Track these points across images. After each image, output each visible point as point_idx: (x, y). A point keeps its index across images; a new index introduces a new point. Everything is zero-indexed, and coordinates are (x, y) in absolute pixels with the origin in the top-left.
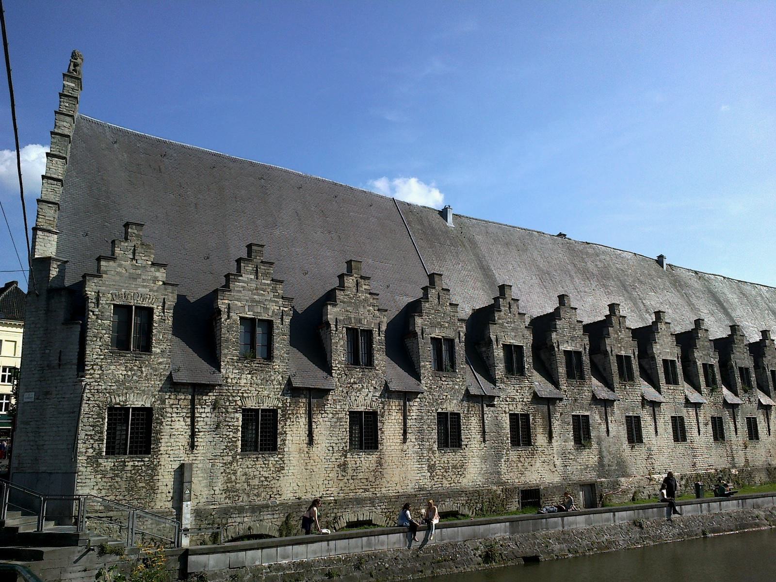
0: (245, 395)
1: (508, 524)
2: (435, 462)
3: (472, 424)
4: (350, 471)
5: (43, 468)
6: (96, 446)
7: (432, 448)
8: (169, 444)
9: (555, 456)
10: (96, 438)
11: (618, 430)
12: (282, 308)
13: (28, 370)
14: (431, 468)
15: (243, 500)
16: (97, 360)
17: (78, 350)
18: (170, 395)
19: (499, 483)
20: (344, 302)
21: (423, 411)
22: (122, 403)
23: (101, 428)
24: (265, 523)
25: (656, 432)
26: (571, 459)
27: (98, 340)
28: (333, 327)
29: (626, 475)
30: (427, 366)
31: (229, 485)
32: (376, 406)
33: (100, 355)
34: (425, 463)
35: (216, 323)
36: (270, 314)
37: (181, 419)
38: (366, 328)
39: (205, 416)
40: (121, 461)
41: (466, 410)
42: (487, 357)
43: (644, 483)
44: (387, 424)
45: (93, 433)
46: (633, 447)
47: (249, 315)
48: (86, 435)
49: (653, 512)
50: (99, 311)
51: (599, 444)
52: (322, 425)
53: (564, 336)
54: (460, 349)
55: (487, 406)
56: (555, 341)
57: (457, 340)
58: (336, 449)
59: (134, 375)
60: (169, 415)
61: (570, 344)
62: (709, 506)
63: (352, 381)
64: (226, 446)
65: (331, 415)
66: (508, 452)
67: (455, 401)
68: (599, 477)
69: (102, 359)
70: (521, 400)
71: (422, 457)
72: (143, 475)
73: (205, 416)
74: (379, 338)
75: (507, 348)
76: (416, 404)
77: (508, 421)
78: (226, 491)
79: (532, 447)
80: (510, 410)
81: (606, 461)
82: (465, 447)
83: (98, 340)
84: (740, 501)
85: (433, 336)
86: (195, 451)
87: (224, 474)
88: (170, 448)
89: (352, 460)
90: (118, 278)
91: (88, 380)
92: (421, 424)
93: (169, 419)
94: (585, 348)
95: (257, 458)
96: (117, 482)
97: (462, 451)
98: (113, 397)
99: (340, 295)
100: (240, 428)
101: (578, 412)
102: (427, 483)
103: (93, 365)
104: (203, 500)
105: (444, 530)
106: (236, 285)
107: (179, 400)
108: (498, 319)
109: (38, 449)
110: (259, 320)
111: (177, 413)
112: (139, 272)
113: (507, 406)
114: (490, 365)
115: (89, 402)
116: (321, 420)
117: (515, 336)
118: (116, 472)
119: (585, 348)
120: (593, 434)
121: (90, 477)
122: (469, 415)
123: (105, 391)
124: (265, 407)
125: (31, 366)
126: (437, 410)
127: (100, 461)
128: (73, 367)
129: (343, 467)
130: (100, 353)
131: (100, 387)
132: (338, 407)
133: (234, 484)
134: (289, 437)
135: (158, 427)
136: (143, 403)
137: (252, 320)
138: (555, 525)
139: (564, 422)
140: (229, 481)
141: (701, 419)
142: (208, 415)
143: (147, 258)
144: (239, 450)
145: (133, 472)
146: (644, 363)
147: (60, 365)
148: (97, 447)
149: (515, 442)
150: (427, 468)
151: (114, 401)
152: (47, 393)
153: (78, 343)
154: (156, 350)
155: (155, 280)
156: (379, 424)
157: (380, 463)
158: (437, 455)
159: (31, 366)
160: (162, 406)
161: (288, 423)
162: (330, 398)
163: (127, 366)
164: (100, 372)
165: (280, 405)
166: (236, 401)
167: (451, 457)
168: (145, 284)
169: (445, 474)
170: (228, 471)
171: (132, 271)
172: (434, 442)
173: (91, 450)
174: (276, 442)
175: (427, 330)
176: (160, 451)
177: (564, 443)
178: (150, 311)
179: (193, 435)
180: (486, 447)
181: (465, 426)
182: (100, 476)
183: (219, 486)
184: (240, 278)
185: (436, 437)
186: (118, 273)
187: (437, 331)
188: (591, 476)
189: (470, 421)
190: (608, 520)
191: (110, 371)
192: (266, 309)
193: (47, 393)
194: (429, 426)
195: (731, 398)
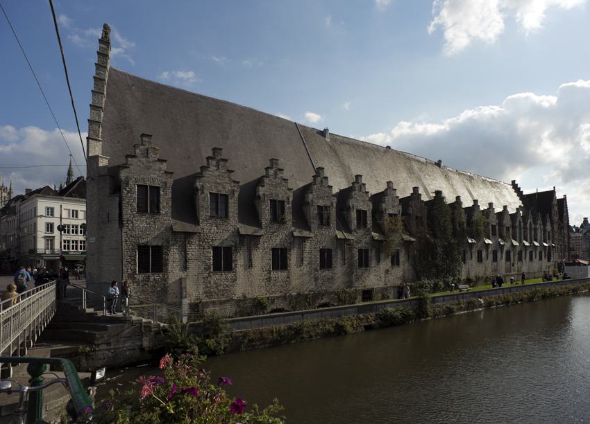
6: (132, 267)
14: (316, 279)
20: (268, 184)
28: (262, 199)
30: (315, 224)
39: (193, 249)
45: (130, 260)
74: (288, 206)
75: (359, 212)
78: (205, 293)
89: (274, 274)
99: (266, 180)
106: (207, 173)
112: (151, 164)
129: (269, 279)
137: (217, 194)
140: (207, 287)
147: (108, 221)
149: (360, 265)
154: (163, 212)
155: (160, 170)
157: (288, 277)
158: (320, 272)
162: (261, 240)
165: (233, 244)
167: (327, 273)
171: (146, 164)
173: (130, 270)
174: (232, 266)
183: (201, 291)
192: (224, 188)
193: (102, 238)
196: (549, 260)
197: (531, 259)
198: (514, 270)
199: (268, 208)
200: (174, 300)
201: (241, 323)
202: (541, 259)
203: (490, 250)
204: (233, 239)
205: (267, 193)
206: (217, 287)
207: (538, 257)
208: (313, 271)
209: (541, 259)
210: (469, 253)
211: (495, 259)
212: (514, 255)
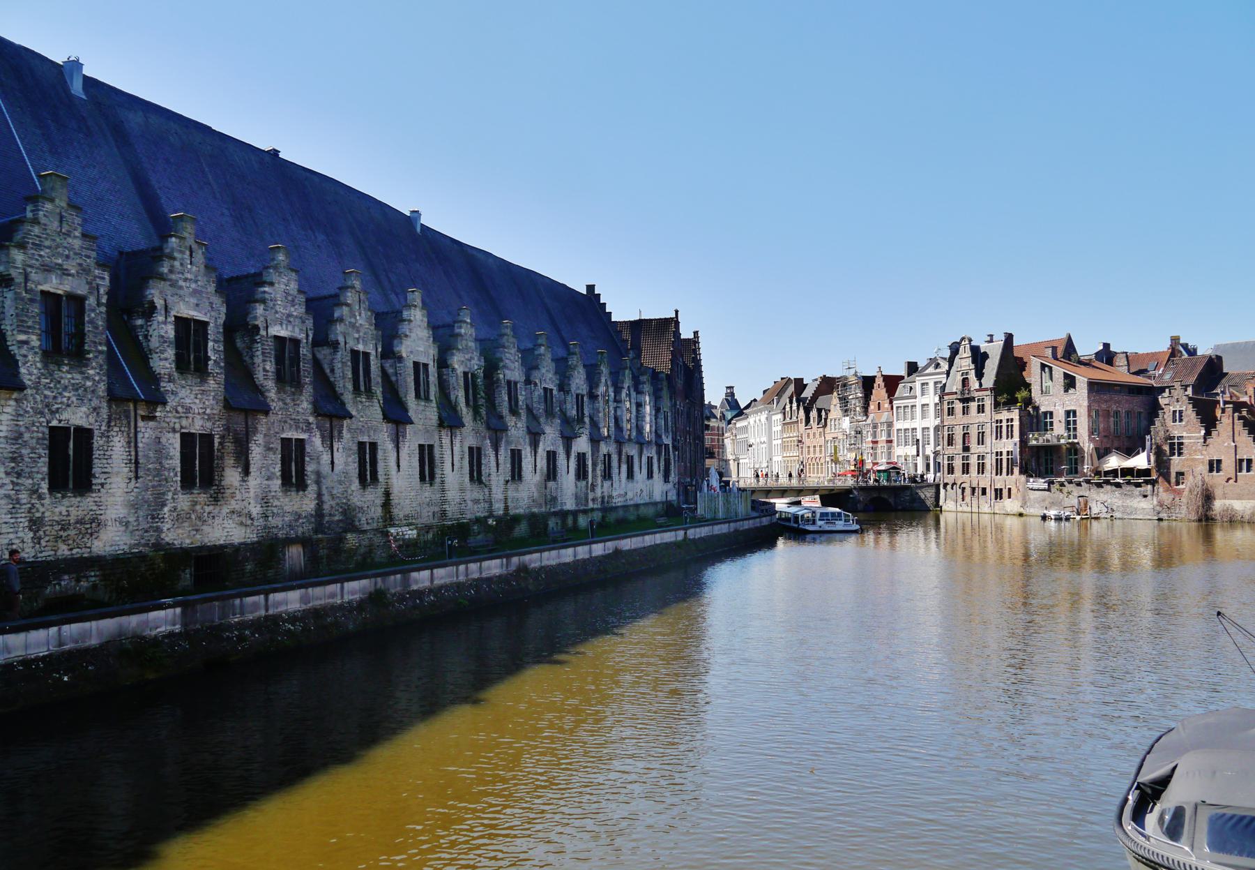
1: (178, 610)
2: (43, 513)
3: (114, 448)
7: (37, 490)
9: (252, 501)
11: (345, 460)
14: (35, 524)
21: (21, 423)
25: (398, 466)
26: (276, 506)
34: (23, 515)
41: (104, 424)
42: (146, 337)
49: (395, 579)
51: (318, 482)
53: (276, 312)
54: (96, 315)
55: (144, 418)
56: (262, 319)
57: (91, 301)
61: (284, 326)
62: (467, 568)
66: (176, 497)
67: (84, 409)
70: (201, 411)
71: (18, 506)
75: (181, 323)
77: (178, 445)
79: (214, 488)
80: (182, 427)
82: (100, 487)
84: (505, 560)
85: (45, 287)
92: (17, 446)
94: (307, 335)
97: (94, 495)
101: (290, 434)
108: (171, 271)
113: (177, 421)
114: (150, 350)
117: (197, 305)
119: (307, 335)
120: (310, 468)
122: (110, 434)
126: (48, 422)
138: (255, 606)
139: (269, 449)
141: (457, 448)
146: (387, 365)
149: (188, 482)
150: (26, 524)
158: (47, 501)
167: (72, 507)
169: (61, 533)
172: (43, 479)
175: (34, 276)
177: (266, 482)
180: (137, 488)
181: (102, 452)
185: (45, 469)
187: (54, 281)
188: (304, 528)
189: (111, 444)
190: (333, 595)
194: (33, 450)
196: (666, 478)
197: (630, 475)
202: (650, 475)
207: (645, 471)
208: (24, 497)
209: (650, 475)
210: (493, 458)
211: (552, 473)
212: (594, 465)
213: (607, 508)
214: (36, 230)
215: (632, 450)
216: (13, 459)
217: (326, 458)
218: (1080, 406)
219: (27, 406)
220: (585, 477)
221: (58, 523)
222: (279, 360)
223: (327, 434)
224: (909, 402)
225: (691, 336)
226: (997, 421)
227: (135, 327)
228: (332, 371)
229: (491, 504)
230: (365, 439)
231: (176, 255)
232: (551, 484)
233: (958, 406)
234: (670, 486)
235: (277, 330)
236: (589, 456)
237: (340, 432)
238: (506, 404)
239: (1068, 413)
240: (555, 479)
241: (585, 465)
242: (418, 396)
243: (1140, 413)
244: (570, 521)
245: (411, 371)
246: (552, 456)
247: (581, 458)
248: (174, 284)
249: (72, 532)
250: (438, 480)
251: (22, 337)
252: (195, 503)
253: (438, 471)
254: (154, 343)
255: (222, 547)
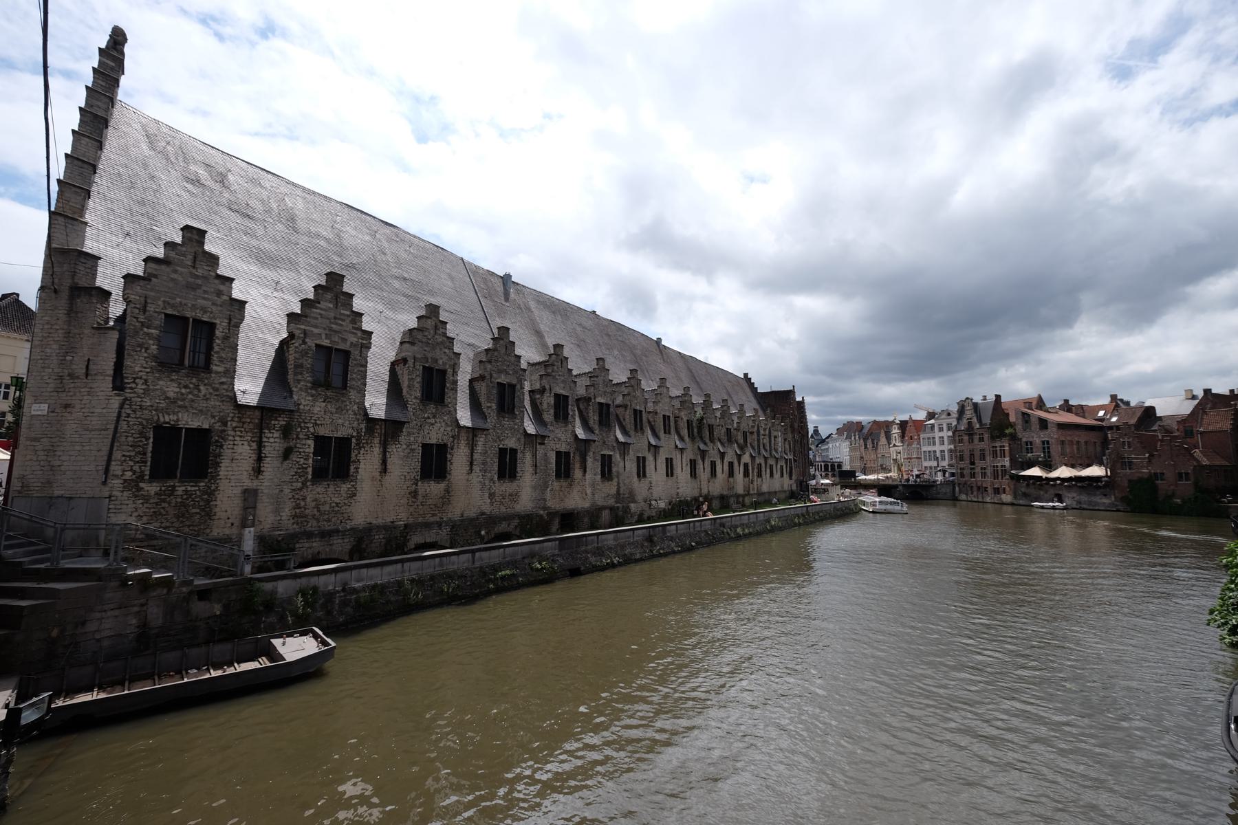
0: (318, 422)
1: (557, 542)
4: (420, 498)
5: (57, 492)
6: (136, 468)
8: (230, 469)
10: (138, 459)
11: (631, 466)
12: (360, 341)
13: (39, 378)
14: (492, 496)
15: (312, 526)
16: (141, 374)
17: (115, 360)
18: (233, 417)
19: (544, 508)
20: (422, 342)
22: (172, 423)
23: (143, 448)
24: (334, 547)
27: (143, 350)
29: (634, 501)
31: (298, 511)
32: (447, 440)
33: (146, 368)
35: (288, 348)
36: (348, 343)
37: (246, 443)
38: (441, 367)
40: (170, 486)
43: (646, 507)
44: (455, 456)
45: (133, 454)
46: (640, 480)
47: (326, 343)
48: (124, 456)
50: (145, 318)
52: (396, 454)
55: (540, 444)
58: (408, 477)
59: (190, 393)
60: (231, 438)
63: (426, 415)
64: (296, 472)
65: (404, 446)
68: (616, 502)
69: (148, 373)
72: (197, 500)
73: (273, 443)
75: (557, 396)
76: (481, 439)
78: (294, 517)
81: (621, 492)
83: (143, 350)
85: (499, 381)
86: (261, 477)
87: (292, 500)
88: (231, 473)
89: (424, 487)
90: (171, 285)
91: (128, 395)
93: (232, 443)
95: (328, 485)
96: (163, 508)
98: (160, 415)
100: (311, 455)
102: (487, 509)
103: (135, 379)
104: (268, 526)
105: (507, 549)
107: (244, 423)
109: (51, 470)
110: (336, 349)
111: (241, 437)
112: (199, 282)
115: (129, 419)
116: (395, 450)
118: (163, 497)
120: (614, 470)
121: (127, 502)
123: (150, 408)
124: (339, 435)
125: (43, 374)
127: (142, 485)
128: (107, 378)
129: (414, 494)
130: (145, 365)
131: (144, 404)
132: (412, 439)
133: (303, 509)
134: (362, 466)
135: (218, 450)
136: (200, 424)
137: (329, 349)
140: (298, 506)
141: (684, 460)
142: (276, 440)
143: (209, 268)
144: (310, 477)
145: (185, 497)
147: (87, 375)
148: (138, 470)
149: (558, 476)
151: (162, 420)
152: (67, 406)
153: (115, 352)
156: (449, 456)
157: (447, 491)
159: (43, 374)
160: (223, 428)
161: (362, 452)
163: (180, 384)
164: (144, 387)
165: (355, 434)
166: (308, 428)
167: (507, 487)
168: (206, 296)
170: (297, 497)
171: (190, 280)
174: (348, 470)
176: (219, 475)
178: (212, 326)
179: (260, 459)
182: (141, 501)
183: (286, 512)
184: (318, 305)
186: (173, 280)
188: (611, 502)
190: (629, 537)
191: (158, 387)
192: (344, 340)
193: (67, 406)
195: (702, 447)
196: (791, 477)
197: (772, 475)
198: (753, 489)
199: (419, 379)
200: (227, 532)
201: (364, 571)
202: (782, 475)
203: (725, 461)
204: (355, 425)
205: (419, 356)
206: (317, 507)
208: (487, 482)
209: (782, 475)
210: (702, 466)
211: (731, 474)
212: (753, 469)
213: (760, 494)
214: (496, 354)
215: (771, 462)
216: (483, 464)
217: (621, 464)
218: (1052, 438)
219: (490, 438)
220: (748, 476)
221: (501, 495)
222: (601, 415)
223: (622, 452)
224: (931, 435)
225: (801, 399)
226: (993, 447)
227: (535, 399)
228: (624, 420)
229: (701, 489)
230: (640, 455)
231: (556, 364)
232: (731, 479)
233: (966, 438)
234: (792, 481)
235: (600, 400)
236: (750, 465)
237: (628, 451)
238: (708, 436)
239: (1043, 442)
240: (733, 476)
241: (748, 470)
242: (665, 432)
243: (1095, 442)
244: (741, 500)
245: (662, 420)
246: (731, 465)
247: (746, 465)
248: (554, 377)
249: (507, 500)
250: (675, 477)
251: (489, 405)
252: (561, 486)
253: (674, 472)
254: (545, 406)
255: (573, 510)
